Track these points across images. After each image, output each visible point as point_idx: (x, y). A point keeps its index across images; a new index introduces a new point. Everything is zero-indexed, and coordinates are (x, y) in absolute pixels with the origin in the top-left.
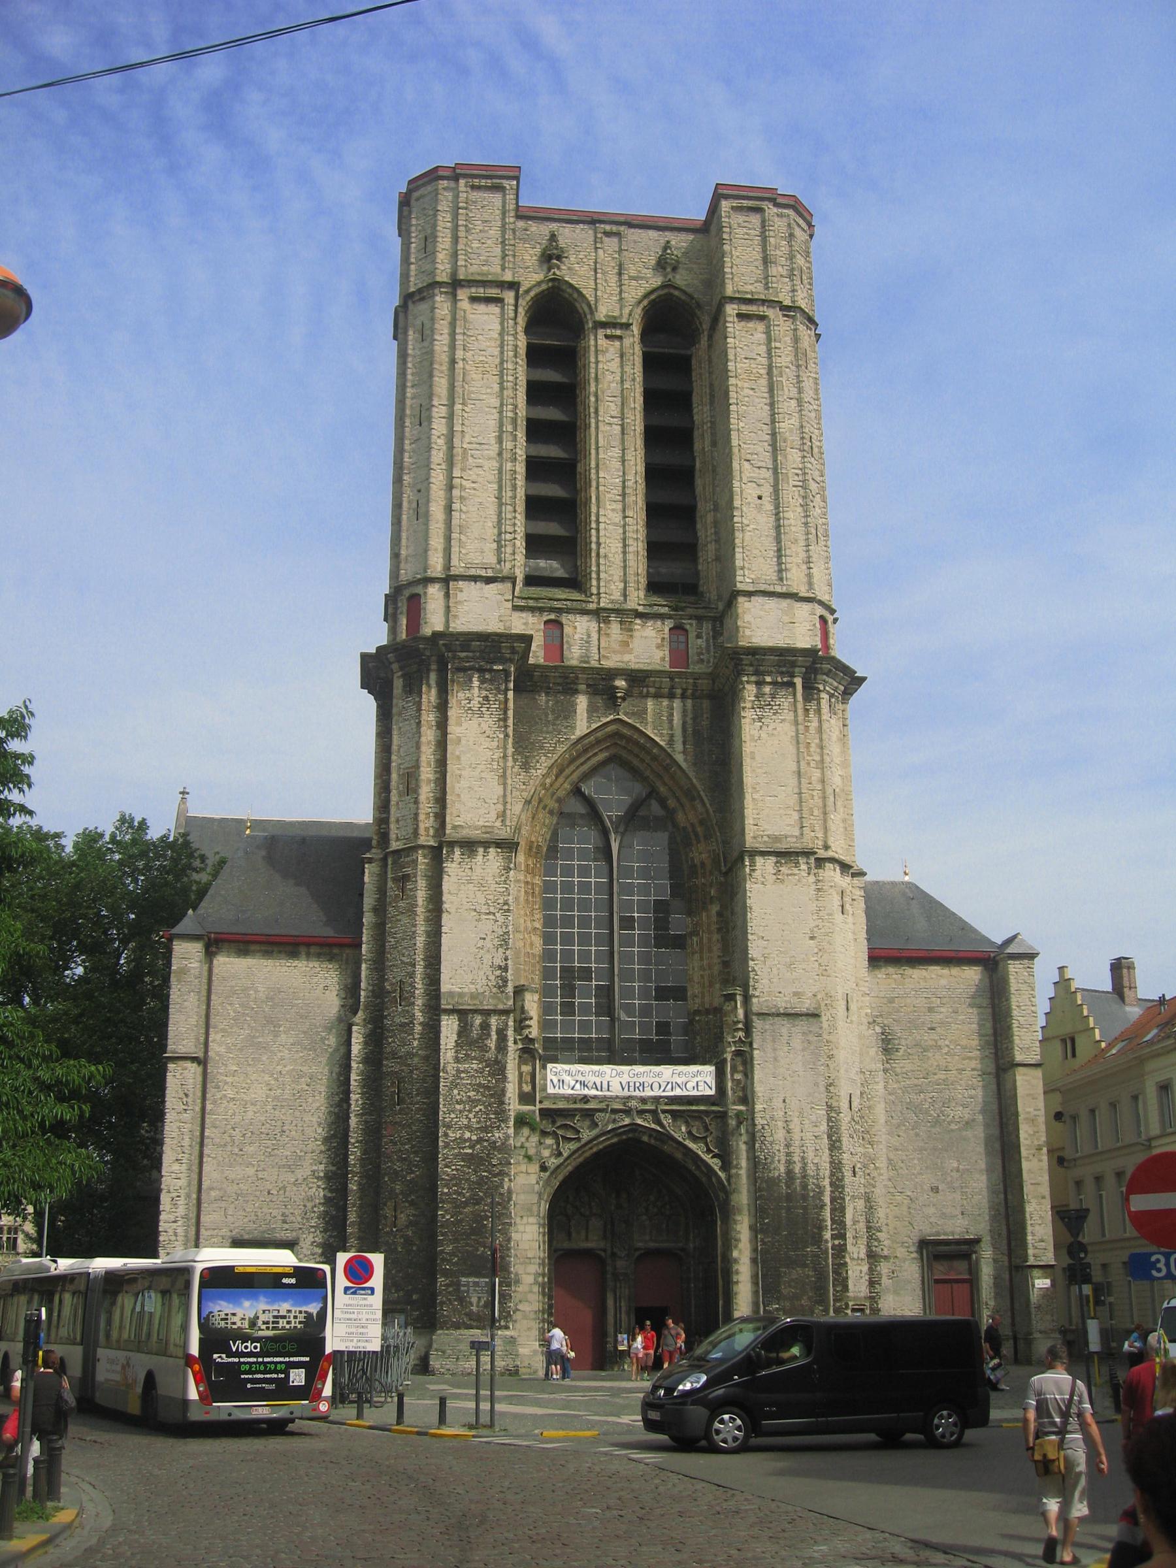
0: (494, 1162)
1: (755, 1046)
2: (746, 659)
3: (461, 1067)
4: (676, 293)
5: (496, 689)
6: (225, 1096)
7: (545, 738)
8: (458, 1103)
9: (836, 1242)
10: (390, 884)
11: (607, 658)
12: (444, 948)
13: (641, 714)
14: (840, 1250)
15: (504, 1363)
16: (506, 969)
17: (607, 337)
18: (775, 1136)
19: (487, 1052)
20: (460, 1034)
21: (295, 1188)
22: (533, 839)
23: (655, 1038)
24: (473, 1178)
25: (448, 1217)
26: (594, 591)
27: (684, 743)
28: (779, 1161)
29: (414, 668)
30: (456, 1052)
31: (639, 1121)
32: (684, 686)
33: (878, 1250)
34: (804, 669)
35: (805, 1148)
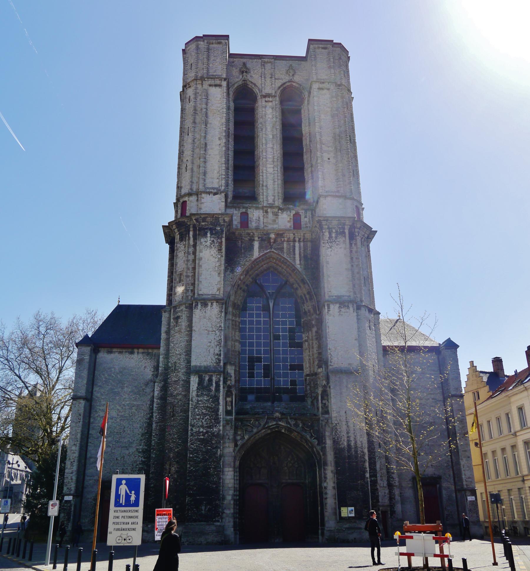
0: (213, 442)
1: (331, 387)
2: (324, 223)
3: (200, 399)
4: (294, 84)
5: (217, 237)
6: (99, 415)
7: (240, 260)
8: (198, 415)
9: (373, 479)
10: (172, 320)
11: (267, 226)
12: (193, 346)
13: (282, 249)
14: (374, 483)
15: (216, 539)
16: (220, 355)
17: (266, 101)
18: (341, 428)
19: (211, 392)
20: (199, 384)
21: (128, 457)
22: (236, 302)
23: (290, 387)
24: (204, 450)
25: (192, 468)
26: (261, 200)
27: (300, 260)
28: (344, 440)
29: (183, 230)
30: (197, 392)
31: (280, 423)
32: (299, 237)
33: (393, 482)
34: (349, 226)
35: (356, 434)
